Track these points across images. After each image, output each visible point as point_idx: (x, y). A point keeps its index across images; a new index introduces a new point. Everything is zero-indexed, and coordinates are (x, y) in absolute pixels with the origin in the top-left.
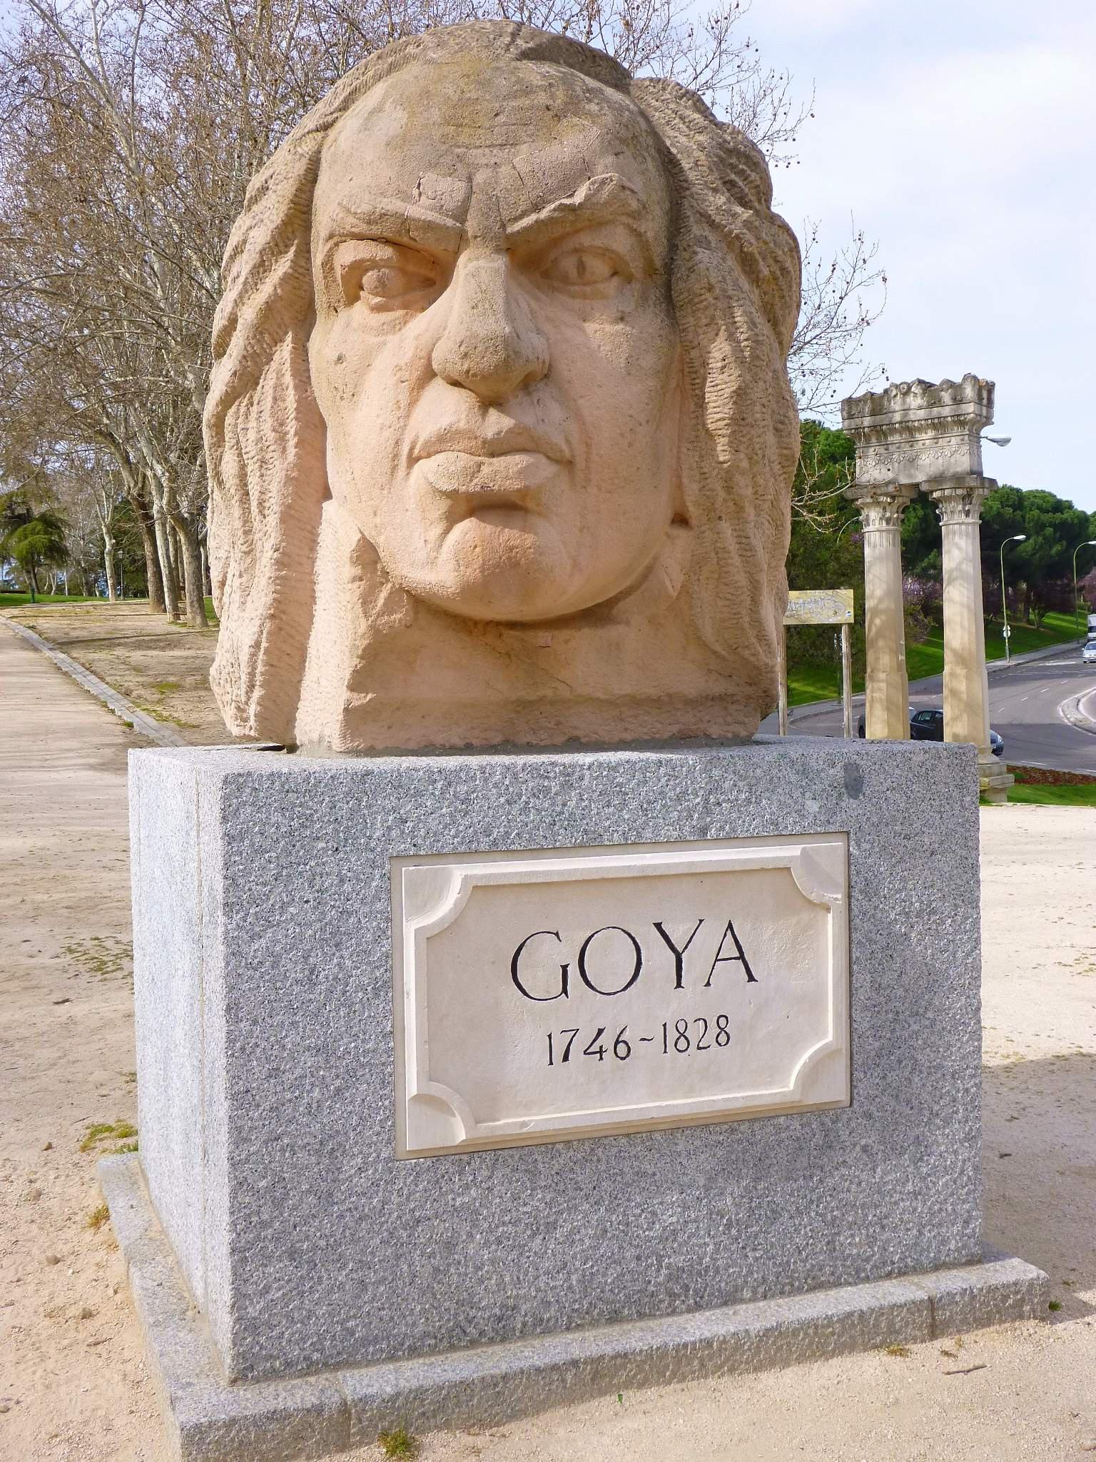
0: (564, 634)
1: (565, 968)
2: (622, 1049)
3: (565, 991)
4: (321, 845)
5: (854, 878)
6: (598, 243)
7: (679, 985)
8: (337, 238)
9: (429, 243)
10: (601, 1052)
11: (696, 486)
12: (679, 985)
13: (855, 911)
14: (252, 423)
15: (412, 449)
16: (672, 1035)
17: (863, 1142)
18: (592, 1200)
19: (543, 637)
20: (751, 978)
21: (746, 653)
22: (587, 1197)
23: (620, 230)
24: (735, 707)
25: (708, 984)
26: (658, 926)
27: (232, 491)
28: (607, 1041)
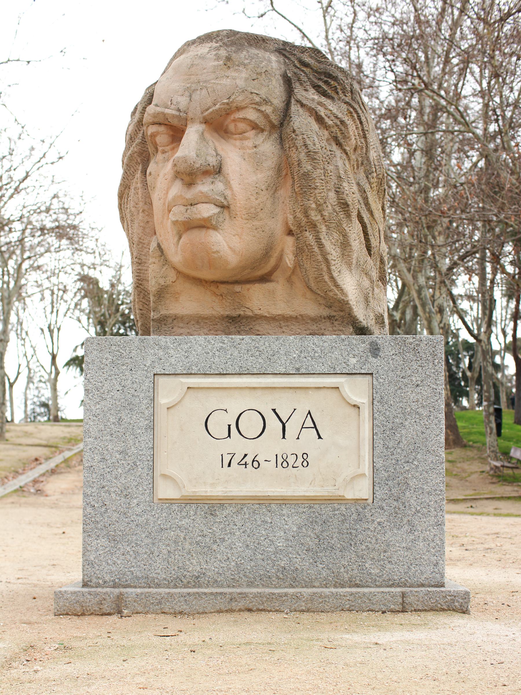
0: (248, 286)
1: (229, 426)
2: (256, 464)
3: (229, 436)
4: (125, 367)
5: (374, 395)
6: (241, 117)
7: (284, 437)
9: (175, 122)
10: (246, 464)
11: (291, 217)
12: (284, 437)
13: (375, 411)
16: (280, 460)
17: (378, 520)
18: (241, 531)
19: (238, 288)
20: (320, 437)
21: (331, 294)
22: (239, 529)
23: (251, 110)
24: (337, 322)
25: (298, 438)
26: (274, 410)
28: (249, 460)
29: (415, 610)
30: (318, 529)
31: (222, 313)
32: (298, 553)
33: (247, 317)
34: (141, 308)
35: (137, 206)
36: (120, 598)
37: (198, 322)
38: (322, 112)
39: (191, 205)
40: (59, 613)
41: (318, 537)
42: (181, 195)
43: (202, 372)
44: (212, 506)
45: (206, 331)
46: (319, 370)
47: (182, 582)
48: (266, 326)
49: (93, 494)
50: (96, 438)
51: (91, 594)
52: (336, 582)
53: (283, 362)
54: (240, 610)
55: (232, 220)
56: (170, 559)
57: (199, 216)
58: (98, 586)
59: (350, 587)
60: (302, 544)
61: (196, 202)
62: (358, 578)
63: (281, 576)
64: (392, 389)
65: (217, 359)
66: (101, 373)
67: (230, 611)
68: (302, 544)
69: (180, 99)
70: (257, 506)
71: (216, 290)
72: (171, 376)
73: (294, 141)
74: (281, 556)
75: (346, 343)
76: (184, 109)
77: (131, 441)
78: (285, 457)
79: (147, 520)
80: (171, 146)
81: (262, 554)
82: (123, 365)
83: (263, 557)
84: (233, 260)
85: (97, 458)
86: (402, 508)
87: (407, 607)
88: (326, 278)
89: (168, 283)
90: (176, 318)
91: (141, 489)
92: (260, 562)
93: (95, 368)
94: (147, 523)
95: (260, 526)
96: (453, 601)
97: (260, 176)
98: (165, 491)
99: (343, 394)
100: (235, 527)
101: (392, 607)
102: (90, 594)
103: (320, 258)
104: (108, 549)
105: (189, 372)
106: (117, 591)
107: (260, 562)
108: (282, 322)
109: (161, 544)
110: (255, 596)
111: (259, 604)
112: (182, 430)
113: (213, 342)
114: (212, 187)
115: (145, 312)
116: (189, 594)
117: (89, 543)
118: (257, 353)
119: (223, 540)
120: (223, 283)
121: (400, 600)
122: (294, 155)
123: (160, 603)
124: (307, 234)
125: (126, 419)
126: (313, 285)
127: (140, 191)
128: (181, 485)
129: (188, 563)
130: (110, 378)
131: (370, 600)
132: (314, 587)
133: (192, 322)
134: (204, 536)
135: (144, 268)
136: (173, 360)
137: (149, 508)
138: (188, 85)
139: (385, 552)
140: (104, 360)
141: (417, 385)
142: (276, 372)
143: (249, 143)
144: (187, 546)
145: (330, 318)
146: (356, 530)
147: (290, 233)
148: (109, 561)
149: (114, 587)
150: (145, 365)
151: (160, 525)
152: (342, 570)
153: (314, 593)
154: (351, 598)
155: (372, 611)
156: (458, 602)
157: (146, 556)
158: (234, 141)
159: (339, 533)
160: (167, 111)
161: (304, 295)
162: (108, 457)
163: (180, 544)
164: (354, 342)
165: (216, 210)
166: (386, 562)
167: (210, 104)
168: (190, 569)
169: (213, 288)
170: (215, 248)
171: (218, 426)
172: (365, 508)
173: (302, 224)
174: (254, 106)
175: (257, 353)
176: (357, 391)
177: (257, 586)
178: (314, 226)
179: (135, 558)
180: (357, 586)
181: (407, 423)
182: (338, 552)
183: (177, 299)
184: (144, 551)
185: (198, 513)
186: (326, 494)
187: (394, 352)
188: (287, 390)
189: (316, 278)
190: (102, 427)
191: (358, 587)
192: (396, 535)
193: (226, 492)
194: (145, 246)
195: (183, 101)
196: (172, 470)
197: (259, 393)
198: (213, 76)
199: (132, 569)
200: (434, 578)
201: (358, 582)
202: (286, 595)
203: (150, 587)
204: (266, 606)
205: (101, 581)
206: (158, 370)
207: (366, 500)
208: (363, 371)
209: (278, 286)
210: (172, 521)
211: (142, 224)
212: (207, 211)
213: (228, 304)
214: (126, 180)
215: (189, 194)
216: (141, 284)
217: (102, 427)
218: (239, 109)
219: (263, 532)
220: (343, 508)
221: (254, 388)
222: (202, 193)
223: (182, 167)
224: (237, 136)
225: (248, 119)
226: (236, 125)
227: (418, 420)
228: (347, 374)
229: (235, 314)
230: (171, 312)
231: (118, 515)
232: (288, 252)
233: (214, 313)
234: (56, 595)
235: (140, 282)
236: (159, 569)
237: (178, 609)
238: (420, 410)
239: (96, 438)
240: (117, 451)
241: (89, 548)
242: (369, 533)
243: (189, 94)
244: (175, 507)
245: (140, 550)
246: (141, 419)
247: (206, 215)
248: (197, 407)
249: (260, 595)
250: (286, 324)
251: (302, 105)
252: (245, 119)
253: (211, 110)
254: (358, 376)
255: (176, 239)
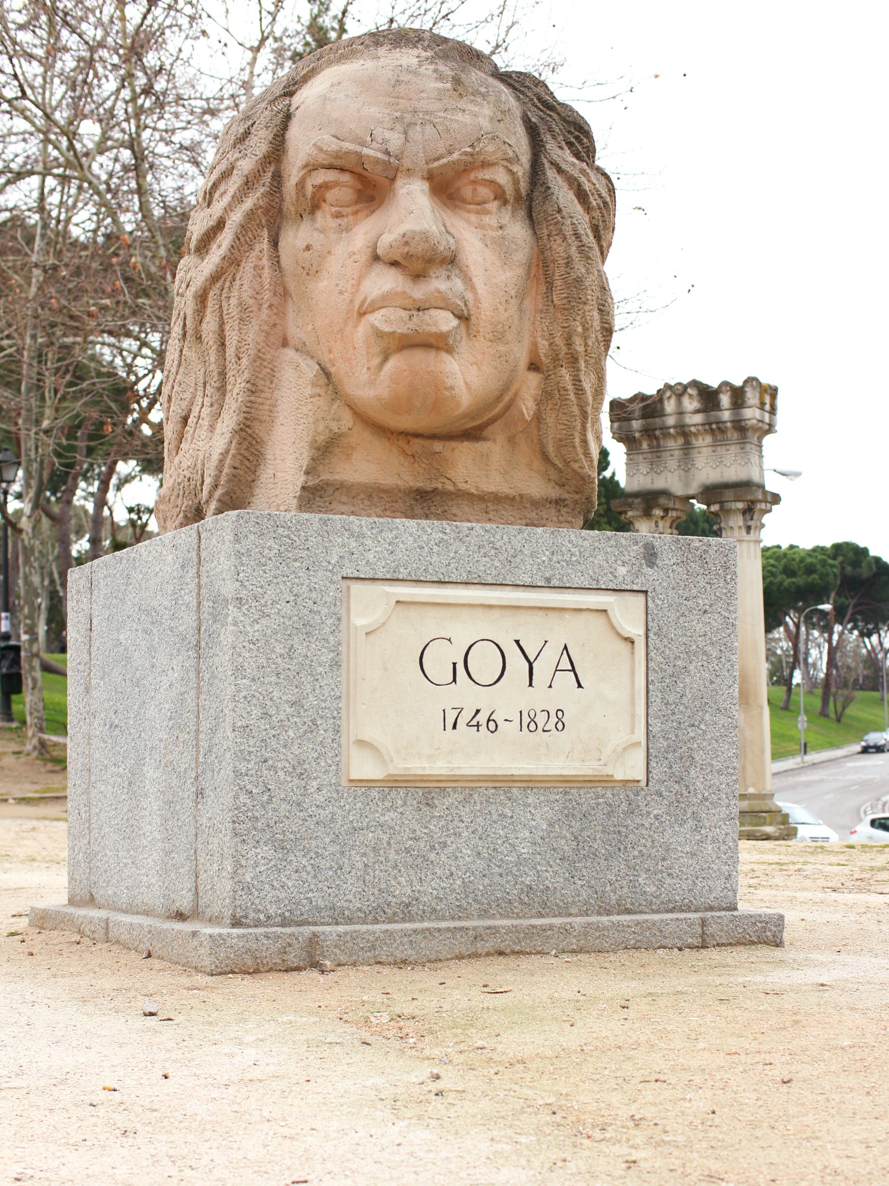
0: (453, 444)
1: (454, 664)
2: (492, 725)
3: (455, 680)
5: (650, 624)
6: (487, 177)
7: (531, 685)
8: (311, 168)
9: (375, 173)
10: (478, 725)
11: (546, 343)
12: (531, 685)
13: (651, 647)
14: (235, 293)
15: (361, 306)
16: (526, 720)
17: (655, 812)
18: (470, 830)
19: (438, 446)
20: (580, 686)
21: (576, 466)
22: (467, 827)
23: (501, 169)
24: (565, 509)
25: (550, 686)
26: (517, 642)
27: (211, 343)
28: (482, 718)
29: (718, 945)
30: (576, 825)
31: (411, 484)
32: (548, 862)
33: (445, 494)
34: (237, 465)
35: (259, 297)
36: (313, 941)
37: (370, 497)
38: (587, 186)
39: (419, 310)
40: (219, 970)
41: (576, 838)
42: (404, 292)
43: (414, 578)
44: (427, 791)
45: (378, 510)
46: (578, 581)
47: (385, 913)
48: (467, 509)
49: (250, 773)
50: (253, 680)
51: (268, 938)
52: (600, 907)
53: (528, 567)
54: (488, 954)
55: (470, 339)
56: (367, 877)
57: (434, 329)
58: (257, 924)
59: (618, 914)
60: (554, 850)
61: (427, 305)
62: (629, 900)
63: (526, 899)
64: (673, 617)
65: (435, 558)
66: (261, 572)
67: (475, 955)
68: (554, 850)
69: (388, 135)
70: (493, 791)
71: (406, 447)
72: (367, 582)
73: (559, 226)
74: (526, 869)
75: (613, 543)
76: (397, 152)
77: (308, 686)
78: (532, 716)
79: (333, 814)
80: (355, 208)
81: (499, 867)
82: (295, 560)
83: (501, 870)
84: (466, 401)
85: (256, 712)
86: (685, 793)
87: (708, 940)
88: (577, 441)
89: (344, 429)
90: (341, 487)
91: (323, 764)
92: (497, 879)
93: (252, 563)
94: (333, 820)
95: (495, 822)
96: (764, 930)
97: (509, 274)
98: (363, 767)
99: (613, 620)
100: (460, 824)
101: (690, 940)
102: (267, 937)
103: (575, 410)
104: (273, 863)
105: (396, 576)
106: (307, 930)
107: (497, 879)
108: (490, 504)
109: (353, 852)
110: (509, 931)
111: (514, 943)
112: (386, 669)
113: (430, 531)
114: (449, 284)
115: (242, 472)
116: (415, 931)
117: (244, 853)
118: (493, 552)
119: (444, 845)
120: (417, 435)
121: (700, 931)
122: (557, 247)
123: (373, 947)
124: (564, 371)
125: (301, 650)
126: (551, 450)
127: (267, 273)
128: (387, 758)
129: (393, 883)
130: (275, 581)
131: (661, 931)
132: (571, 915)
133: (362, 496)
134: (416, 839)
135: (259, 400)
136: (370, 556)
137: (335, 795)
138: (398, 114)
139: (664, 859)
140: (267, 551)
141: (705, 612)
142: (518, 582)
143: (491, 220)
144: (392, 856)
145: (558, 502)
146: (627, 827)
147: (534, 366)
148: (275, 883)
149: (283, 925)
150: (329, 563)
151: (352, 822)
152: (608, 888)
153: (589, 924)
154: (637, 929)
155: (665, 947)
156: (770, 930)
157: (331, 873)
158: (467, 215)
159: (604, 832)
160: (366, 151)
161: (529, 465)
162: (272, 711)
163: (382, 852)
164: (624, 542)
165: (455, 322)
166: (665, 875)
167: (441, 151)
168: (397, 892)
169: (402, 443)
170: (449, 382)
171: (439, 663)
172: (637, 794)
173: (561, 356)
174: (506, 163)
175: (493, 552)
176: (629, 615)
177: (493, 917)
178: (574, 359)
179: (315, 877)
180: (628, 912)
181: (692, 668)
182: (602, 861)
183: (348, 457)
184: (328, 865)
185: (408, 803)
186: (590, 772)
187: (674, 560)
188: (536, 612)
189: (561, 440)
190: (262, 661)
191: (629, 913)
192: (676, 834)
193: (453, 769)
194: (265, 364)
195: (395, 140)
196: (369, 733)
197: (497, 613)
198: (438, 105)
199: (310, 895)
200: (726, 897)
201: (628, 906)
202: (551, 927)
203: (337, 924)
204: (524, 946)
205: (262, 917)
206: (349, 571)
207: (638, 781)
208: (635, 588)
209: (494, 448)
210: (371, 817)
211: (265, 328)
212: (446, 322)
213: (422, 471)
214: (236, 251)
215: (419, 292)
216: (249, 427)
217: (262, 661)
218: (485, 165)
219: (501, 832)
220: (609, 794)
221: (490, 607)
222: (440, 292)
223: (420, 248)
224: (472, 207)
225: (496, 183)
226: (475, 190)
227: (705, 664)
228: (614, 590)
229: (429, 486)
230: (337, 477)
231: (288, 807)
232: (527, 396)
233: (399, 482)
234: (213, 941)
235: (248, 423)
236: (350, 894)
237: (400, 956)
238: (709, 649)
239: (253, 680)
240: (287, 701)
241: (243, 863)
242: (644, 832)
243: (402, 129)
244: (374, 793)
245: (323, 864)
246: (323, 650)
247: (445, 328)
248: (412, 632)
249: (516, 929)
250: (496, 507)
251: (560, 170)
252: (492, 182)
253: (445, 161)
254: (627, 594)
255: (376, 361)
